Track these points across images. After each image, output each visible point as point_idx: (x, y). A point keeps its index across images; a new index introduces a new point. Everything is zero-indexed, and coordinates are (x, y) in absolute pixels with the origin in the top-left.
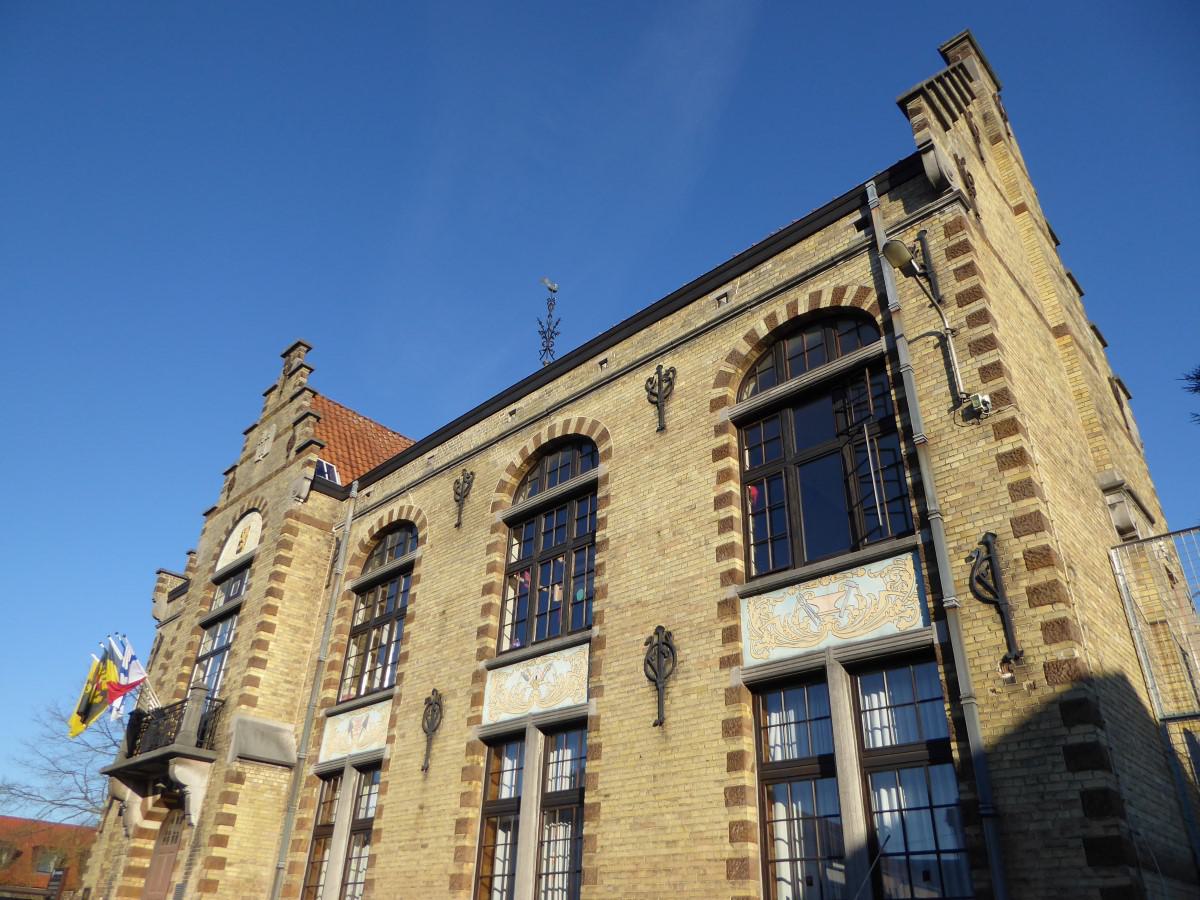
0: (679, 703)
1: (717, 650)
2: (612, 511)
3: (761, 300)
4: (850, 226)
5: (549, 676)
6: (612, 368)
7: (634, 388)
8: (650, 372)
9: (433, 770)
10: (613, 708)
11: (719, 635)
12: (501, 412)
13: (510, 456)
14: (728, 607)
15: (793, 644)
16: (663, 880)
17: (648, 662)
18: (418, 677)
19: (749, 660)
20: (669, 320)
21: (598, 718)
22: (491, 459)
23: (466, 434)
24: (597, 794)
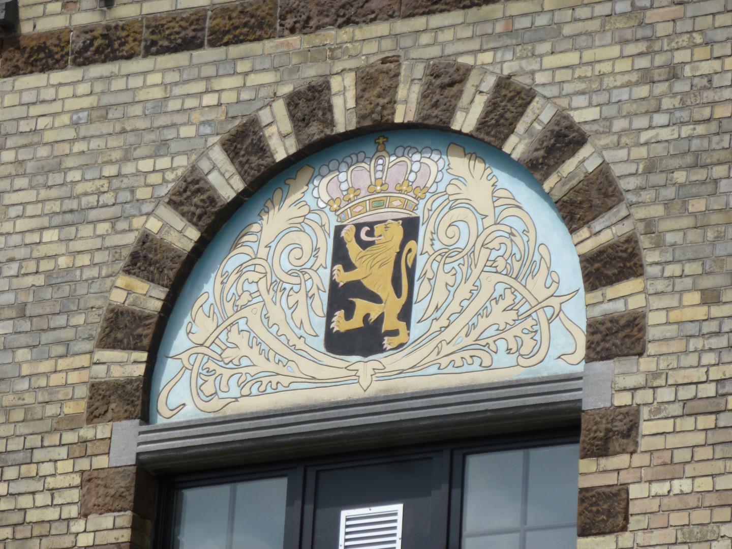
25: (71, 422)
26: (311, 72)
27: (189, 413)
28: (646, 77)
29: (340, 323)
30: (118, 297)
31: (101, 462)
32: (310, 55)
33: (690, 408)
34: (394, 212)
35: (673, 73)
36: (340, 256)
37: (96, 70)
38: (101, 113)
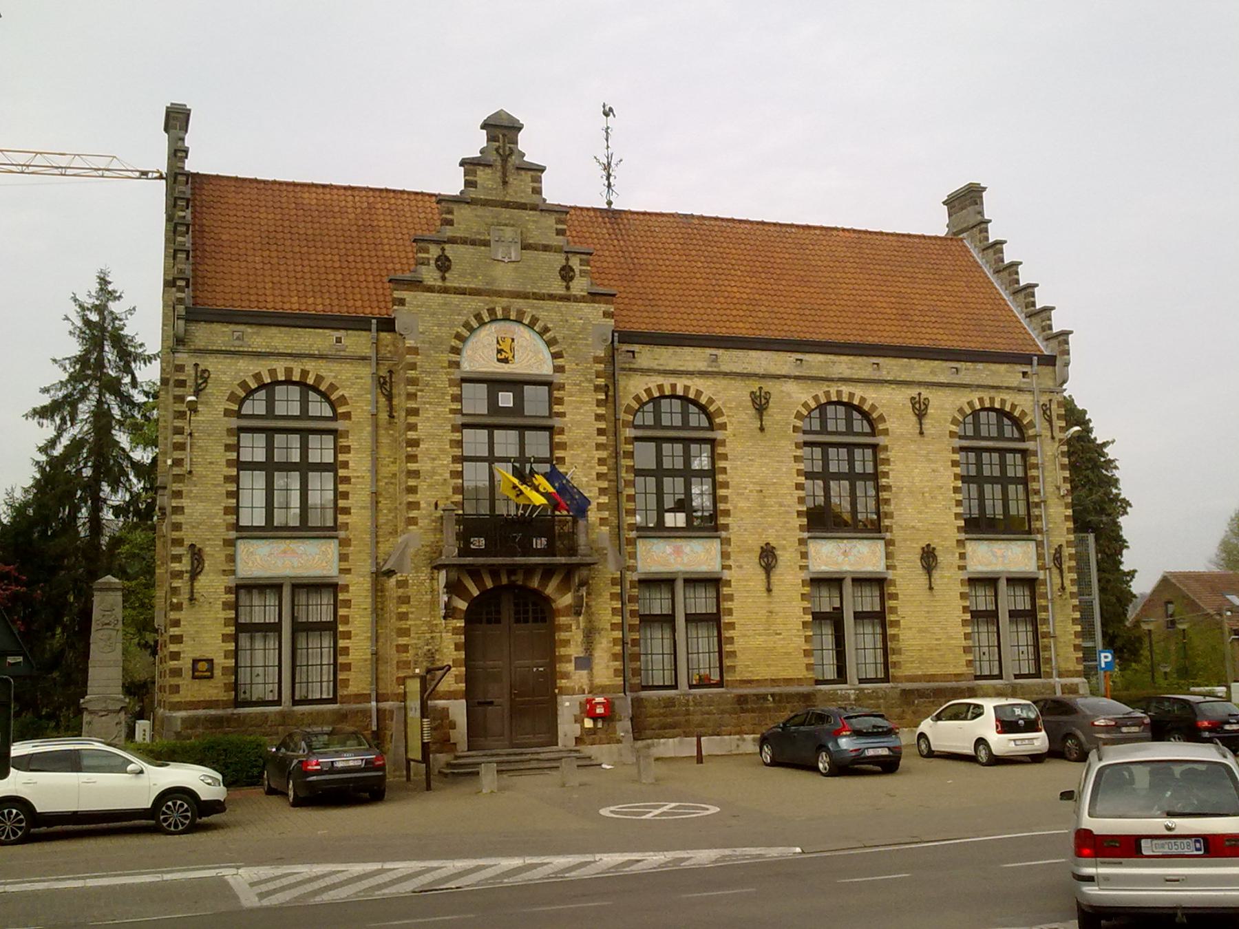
0: (939, 582)
1: (956, 560)
2: (892, 470)
3: (980, 387)
5: (855, 551)
6: (884, 375)
7: (902, 397)
8: (913, 392)
11: (957, 555)
12: (789, 354)
13: (802, 395)
14: (960, 543)
15: (986, 565)
16: (935, 653)
17: (922, 558)
18: (745, 530)
19: (970, 569)
20: (922, 363)
21: (895, 580)
22: (784, 388)
23: (753, 354)
24: (898, 616)
25: (445, 368)
26: (492, 306)
27: (468, 369)
28: (562, 321)
29: (499, 356)
30: (453, 344)
32: (492, 302)
33: (575, 384)
34: (509, 336)
35: (567, 321)
36: (498, 342)
37: (443, 295)
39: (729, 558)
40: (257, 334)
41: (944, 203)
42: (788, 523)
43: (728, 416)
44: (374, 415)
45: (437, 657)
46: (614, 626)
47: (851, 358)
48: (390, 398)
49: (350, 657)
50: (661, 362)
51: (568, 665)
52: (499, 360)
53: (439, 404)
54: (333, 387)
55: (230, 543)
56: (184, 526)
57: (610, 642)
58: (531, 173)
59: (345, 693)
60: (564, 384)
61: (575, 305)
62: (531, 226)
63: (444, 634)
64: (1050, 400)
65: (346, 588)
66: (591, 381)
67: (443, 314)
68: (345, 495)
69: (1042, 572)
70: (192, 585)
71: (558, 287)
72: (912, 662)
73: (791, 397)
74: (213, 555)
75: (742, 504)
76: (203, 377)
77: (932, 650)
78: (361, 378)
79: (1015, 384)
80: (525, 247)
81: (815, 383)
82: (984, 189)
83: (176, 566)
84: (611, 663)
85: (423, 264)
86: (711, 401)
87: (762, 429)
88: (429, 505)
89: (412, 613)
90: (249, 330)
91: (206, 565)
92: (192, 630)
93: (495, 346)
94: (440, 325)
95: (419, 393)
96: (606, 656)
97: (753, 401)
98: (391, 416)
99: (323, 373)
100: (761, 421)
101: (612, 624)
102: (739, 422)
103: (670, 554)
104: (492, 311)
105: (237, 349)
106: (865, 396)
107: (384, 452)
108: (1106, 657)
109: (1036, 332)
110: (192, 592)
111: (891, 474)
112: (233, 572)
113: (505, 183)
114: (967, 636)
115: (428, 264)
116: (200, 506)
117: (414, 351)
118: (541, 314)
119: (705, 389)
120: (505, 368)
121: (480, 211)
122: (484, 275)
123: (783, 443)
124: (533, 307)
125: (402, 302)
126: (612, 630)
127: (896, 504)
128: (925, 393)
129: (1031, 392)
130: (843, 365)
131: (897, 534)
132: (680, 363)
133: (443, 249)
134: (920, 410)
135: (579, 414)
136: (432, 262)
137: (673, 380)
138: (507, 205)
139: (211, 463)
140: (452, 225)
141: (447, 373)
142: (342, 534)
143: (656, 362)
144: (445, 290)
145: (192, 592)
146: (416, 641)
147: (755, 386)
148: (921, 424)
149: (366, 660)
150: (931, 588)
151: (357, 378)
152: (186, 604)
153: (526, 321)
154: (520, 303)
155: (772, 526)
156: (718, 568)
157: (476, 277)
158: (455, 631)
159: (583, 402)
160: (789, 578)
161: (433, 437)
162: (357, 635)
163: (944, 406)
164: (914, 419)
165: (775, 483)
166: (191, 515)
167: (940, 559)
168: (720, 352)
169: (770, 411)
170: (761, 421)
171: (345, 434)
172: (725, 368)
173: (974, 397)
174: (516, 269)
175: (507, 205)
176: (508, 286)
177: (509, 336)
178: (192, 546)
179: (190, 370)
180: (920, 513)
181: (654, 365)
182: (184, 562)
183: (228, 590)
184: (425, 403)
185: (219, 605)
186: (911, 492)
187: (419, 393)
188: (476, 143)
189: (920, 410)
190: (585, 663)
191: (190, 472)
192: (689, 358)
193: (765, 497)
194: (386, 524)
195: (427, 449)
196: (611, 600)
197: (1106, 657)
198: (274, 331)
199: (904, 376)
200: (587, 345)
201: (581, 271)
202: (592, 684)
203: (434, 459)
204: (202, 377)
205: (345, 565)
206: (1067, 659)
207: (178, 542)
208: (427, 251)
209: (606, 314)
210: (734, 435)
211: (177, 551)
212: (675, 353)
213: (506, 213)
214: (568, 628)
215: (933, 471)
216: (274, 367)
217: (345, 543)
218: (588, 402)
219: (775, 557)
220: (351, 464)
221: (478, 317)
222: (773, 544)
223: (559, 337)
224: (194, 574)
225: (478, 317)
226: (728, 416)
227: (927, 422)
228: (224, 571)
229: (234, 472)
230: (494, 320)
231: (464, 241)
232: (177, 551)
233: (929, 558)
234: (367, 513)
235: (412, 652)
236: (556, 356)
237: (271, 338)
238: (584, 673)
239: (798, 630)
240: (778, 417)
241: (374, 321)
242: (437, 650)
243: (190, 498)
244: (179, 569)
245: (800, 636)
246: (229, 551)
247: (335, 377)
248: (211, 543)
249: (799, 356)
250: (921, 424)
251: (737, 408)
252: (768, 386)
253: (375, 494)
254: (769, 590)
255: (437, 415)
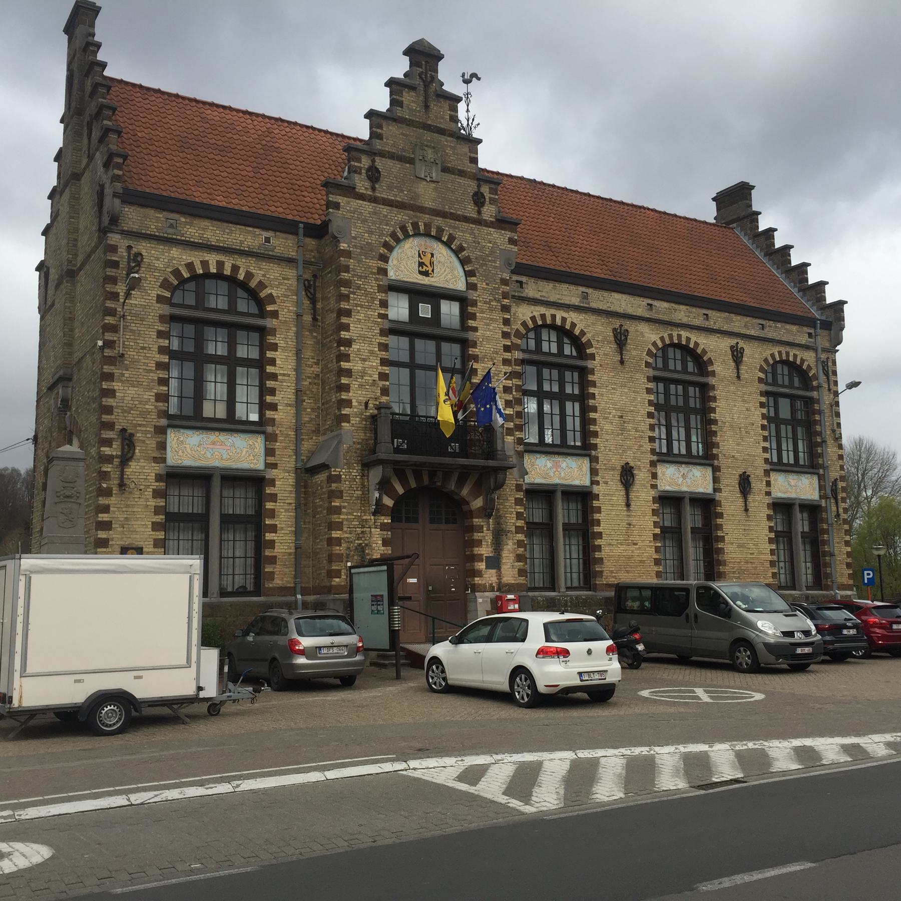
1: (764, 489)
4: (806, 333)
5: (690, 475)
6: (711, 324)
8: (733, 341)
9: (633, 507)
10: (726, 499)
16: (750, 565)
18: (610, 450)
20: (739, 318)
23: (616, 296)
25: (373, 273)
27: (393, 278)
28: (474, 242)
30: (382, 252)
31: (381, 283)
32: (416, 217)
33: (485, 303)
34: (429, 250)
35: (479, 243)
36: (419, 256)
37: (373, 204)
38: (375, 213)
39: (597, 475)
40: (191, 225)
41: (714, 199)
42: (642, 446)
43: (596, 348)
44: (299, 316)
45: (367, 551)
46: (518, 530)
47: (688, 307)
48: (313, 301)
49: (276, 551)
50: (544, 294)
51: (480, 564)
52: (421, 273)
53: (369, 308)
54: (262, 286)
55: (161, 431)
56: (115, 410)
57: (514, 544)
58: (448, 102)
59: (271, 585)
60: (476, 301)
61: (485, 230)
62: (449, 151)
63: (373, 530)
64: (828, 358)
65: (272, 482)
66: (498, 301)
67: (374, 223)
68: (272, 392)
69: (823, 501)
70: (122, 473)
71: (470, 210)
72: (734, 573)
73: (643, 337)
74: (144, 442)
75: (607, 427)
76: (137, 260)
77: (747, 562)
78: (288, 279)
79: (803, 342)
80: (445, 170)
81: (661, 326)
82: (753, 187)
83: (106, 450)
84: (516, 564)
85: (355, 172)
86: (583, 333)
87: (622, 362)
88: (360, 403)
89: (344, 507)
90: (183, 220)
91: (137, 451)
92: (121, 517)
93: (417, 259)
94: (371, 233)
95: (352, 296)
96: (512, 557)
97: (615, 337)
98: (315, 319)
99: (253, 271)
100: (622, 355)
101: (516, 527)
102: (604, 354)
103: (551, 468)
104: (415, 225)
105: (170, 236)
106: (698, 341)
107: (308, 353)
108: (868, 574)
109: (810, 303)
110: (122, 478)
111: (718, 410)
112: (164, 460)
113: (427, 107)
114: (772, 552)
115: (360, 173)
116: (132, 391)
117: (348, 254)
118: (458, 234)
119: (579, 322)
120: (425, 281)
121: (405, 130)
122: (409, 191)
123: (638, 376)
124: (454, 228)
125: (337, 206)
126: (516, 533)
127: (721, 436)
128: (741, 344)
129: (815, 350)
130: (682, 314)
131: (722, 462)
132: (559, 297)
133: (373, 161)
134: (737, 356)
135: (489, 330)
136: (363, 171)
137: (553, 311)
138: (428, 128)
139: (143, 348)
140: (381, 139)
141: (376, 279)
142: (269, 429)
143: (540, 294)
144: (374, 200)
145: (122, 478)
146: (346, 535)
147: (617, 323)
148: (738, 369)
149: (290, 554)
150: (746, 510)
151: (284, 279)
152: (115, 490)
153: (445, 239)
154: (439, 221)
155: (630, 448)
156: (588, 483)
157: (402, 191)
158: (383, 527)
159: (492, 319)
160: (643, 496)
161: (364, 338)
162: (282, 529)
163: (754, 355)
164: (733, 364)
165: (632, 411)
166: (123, 398)
167: (753, 485)
168: (590, 291)
169: (628, 347)
170: (622, 355)
171: (273, 332)
172: (593, 305)
173: (776, 350)
174: (435, 189)
175: (428, 128)
176: (429, 204)
177: (429, 250)
178: (124, 430)
179: (122, 252)
180: (738, 445)
181: (538, 296)
182: (114, 446)
183: (159, 478)
184: (357, 305)
185: (149, 493)
186: (732, 426)
187: (352, 296)
188: (400, 68)
189: (737, 356)
190: (494, 562)
191: (122, 356)
192: (566, 293)
193: (624, 422)
194: (309, 422)
195: (359, 350)
196: (516, 505)
197: (868, 574)
198: (206, 223)
199: (726, 327)
200: (495, 267)
201: (490, 198)
202: (500, 582)
203: (364, 360)
204: (135, 260)
205: (271, 460)
206: (842, 575)
207: (110, 426)
208: (359, 161)
209: (512, 241)
210: (601, 366)
211: (107, 434)
212: (554, 288)
213: (428, 136)
214: (480, 529)
215: (747, 410)
216: (207, 259)
217: (270, 438)
218: (496, 320)
219: (633, 476)
220: (278, 362)
221: (403, 229)
222: (632, 464)
223: (472, 256)
224: (125, 459)
225: (403, 229)
226: (596, 348)
227: (743, 368)
228: (155, 458)
229: (165, 359)
230: (417, 234)
231: (392, 156)
232: (107, 434)
233: (745, 484)
234: (292, 411)
235: (344, 545)
236: (468, 274)
237: (204, 229)
238: (493, 571)
239: (650, 542)
240: (634, 353)
241: (301, 225)
242: (367, 545)
243: (122, 381)
244: (110, 453)
245: (651, 547)
246: (160, 439)
247: (264, 276)
248: (144, 429)
249: (650, 302)
250: (738, 369)
251: (603, 342)
252: (628, 325)
253: (298, 392)
254: (628, 505)
255: (368, 318)
